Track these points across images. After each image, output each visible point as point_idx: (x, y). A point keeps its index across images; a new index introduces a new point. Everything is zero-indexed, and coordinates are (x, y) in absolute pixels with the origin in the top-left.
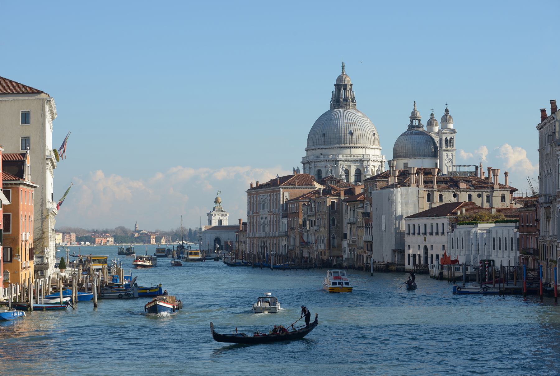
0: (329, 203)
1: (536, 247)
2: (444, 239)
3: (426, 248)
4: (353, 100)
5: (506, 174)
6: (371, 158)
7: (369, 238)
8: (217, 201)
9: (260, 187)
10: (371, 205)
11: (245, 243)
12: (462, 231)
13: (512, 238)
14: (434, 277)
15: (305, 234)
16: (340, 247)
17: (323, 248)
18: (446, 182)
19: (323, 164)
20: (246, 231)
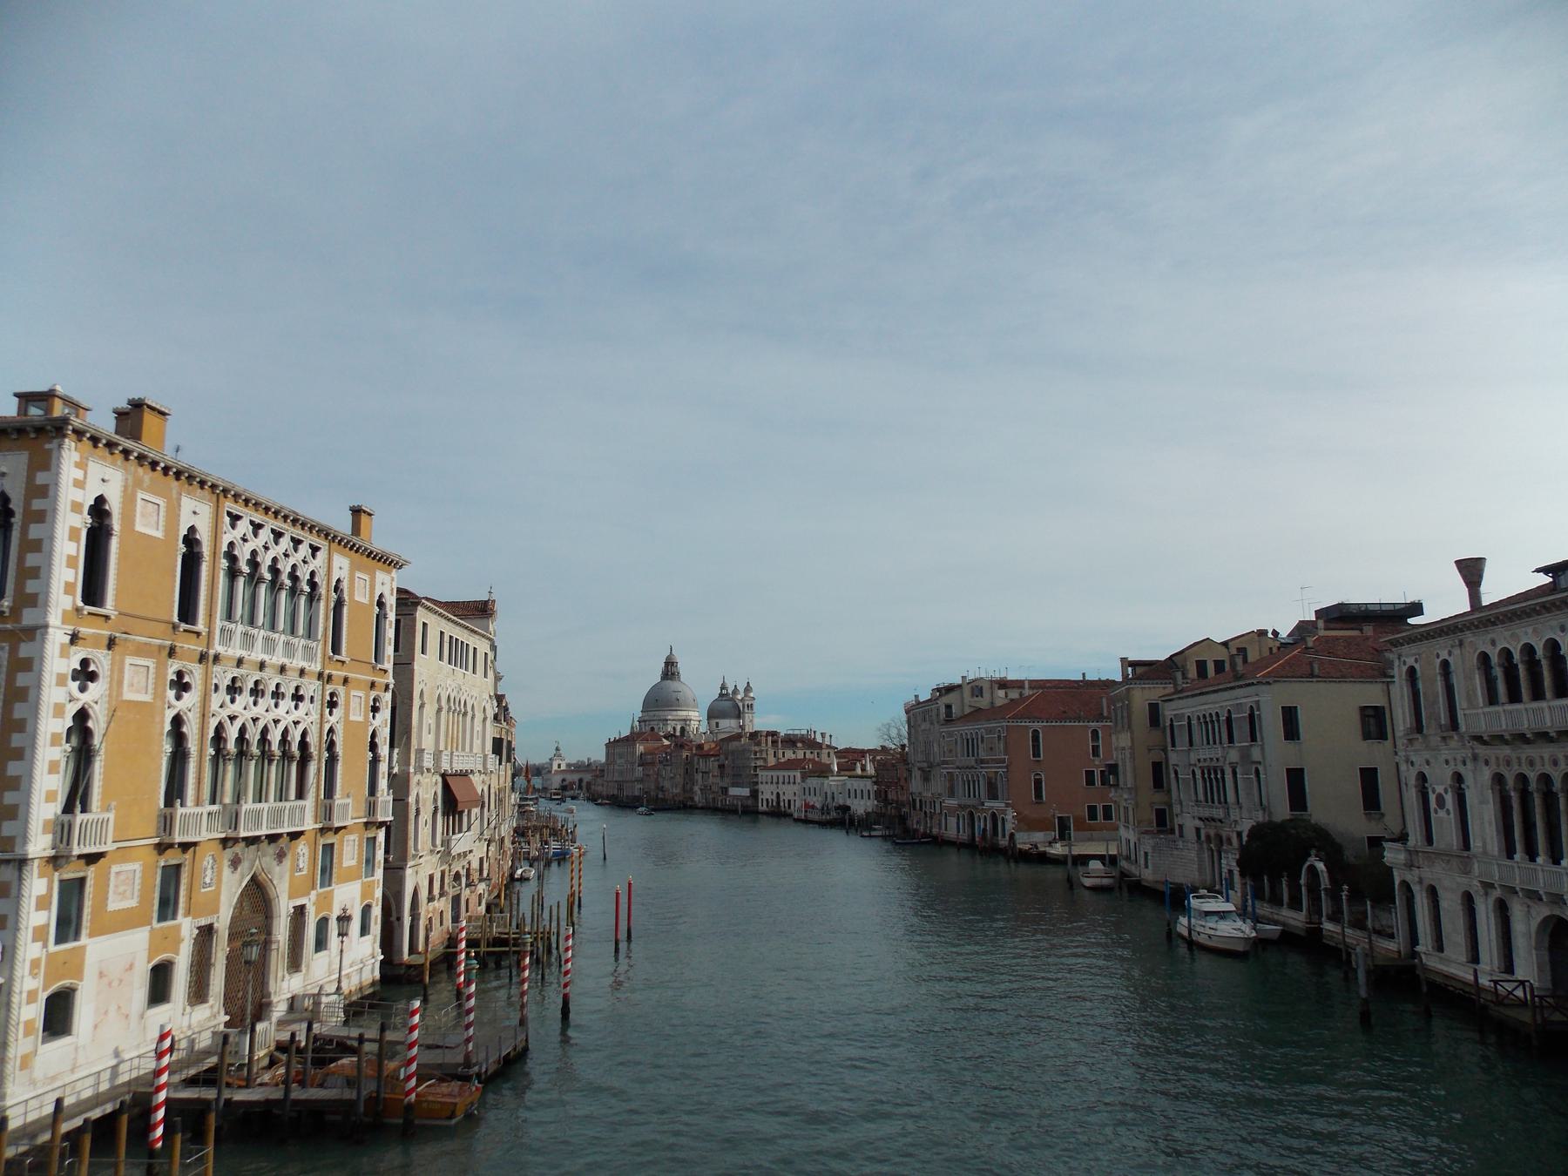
0: (684, 756)
1: (895, 798)
2: (796, 788)
3: (778, 794)
4: (678, 673)
5: (831, 736)
6: (693, 718)
7: (726, 786)
8: (557, 749)
9: (616, 741)
10: (727, 759)
11: (603, 785)
12: (815, 782)
13: (869, 791)
14: (798, 820)
15: (660, 779)
16: (691, 789)
17: (678, 791)
18: (787, 742)
19: (656, 722)
20: (603, 776)
